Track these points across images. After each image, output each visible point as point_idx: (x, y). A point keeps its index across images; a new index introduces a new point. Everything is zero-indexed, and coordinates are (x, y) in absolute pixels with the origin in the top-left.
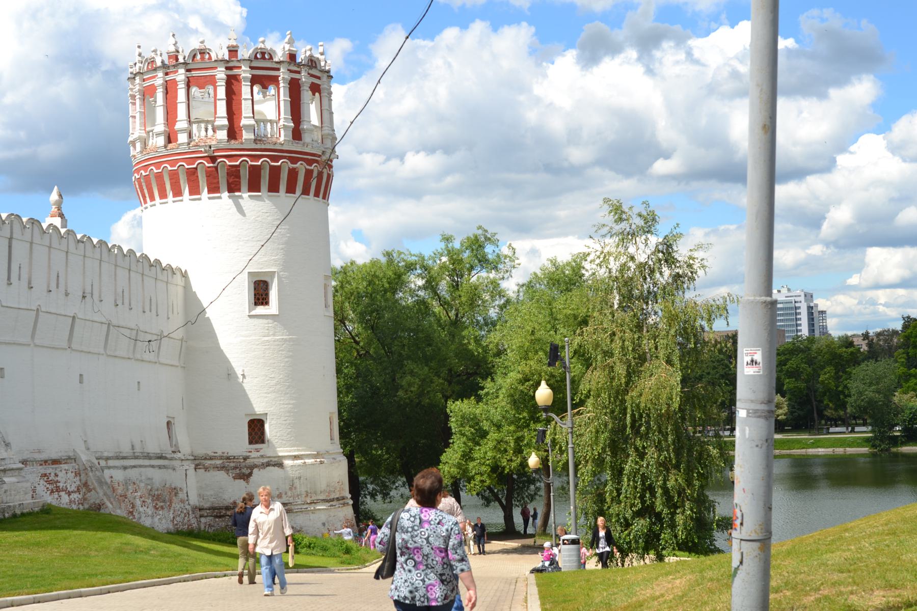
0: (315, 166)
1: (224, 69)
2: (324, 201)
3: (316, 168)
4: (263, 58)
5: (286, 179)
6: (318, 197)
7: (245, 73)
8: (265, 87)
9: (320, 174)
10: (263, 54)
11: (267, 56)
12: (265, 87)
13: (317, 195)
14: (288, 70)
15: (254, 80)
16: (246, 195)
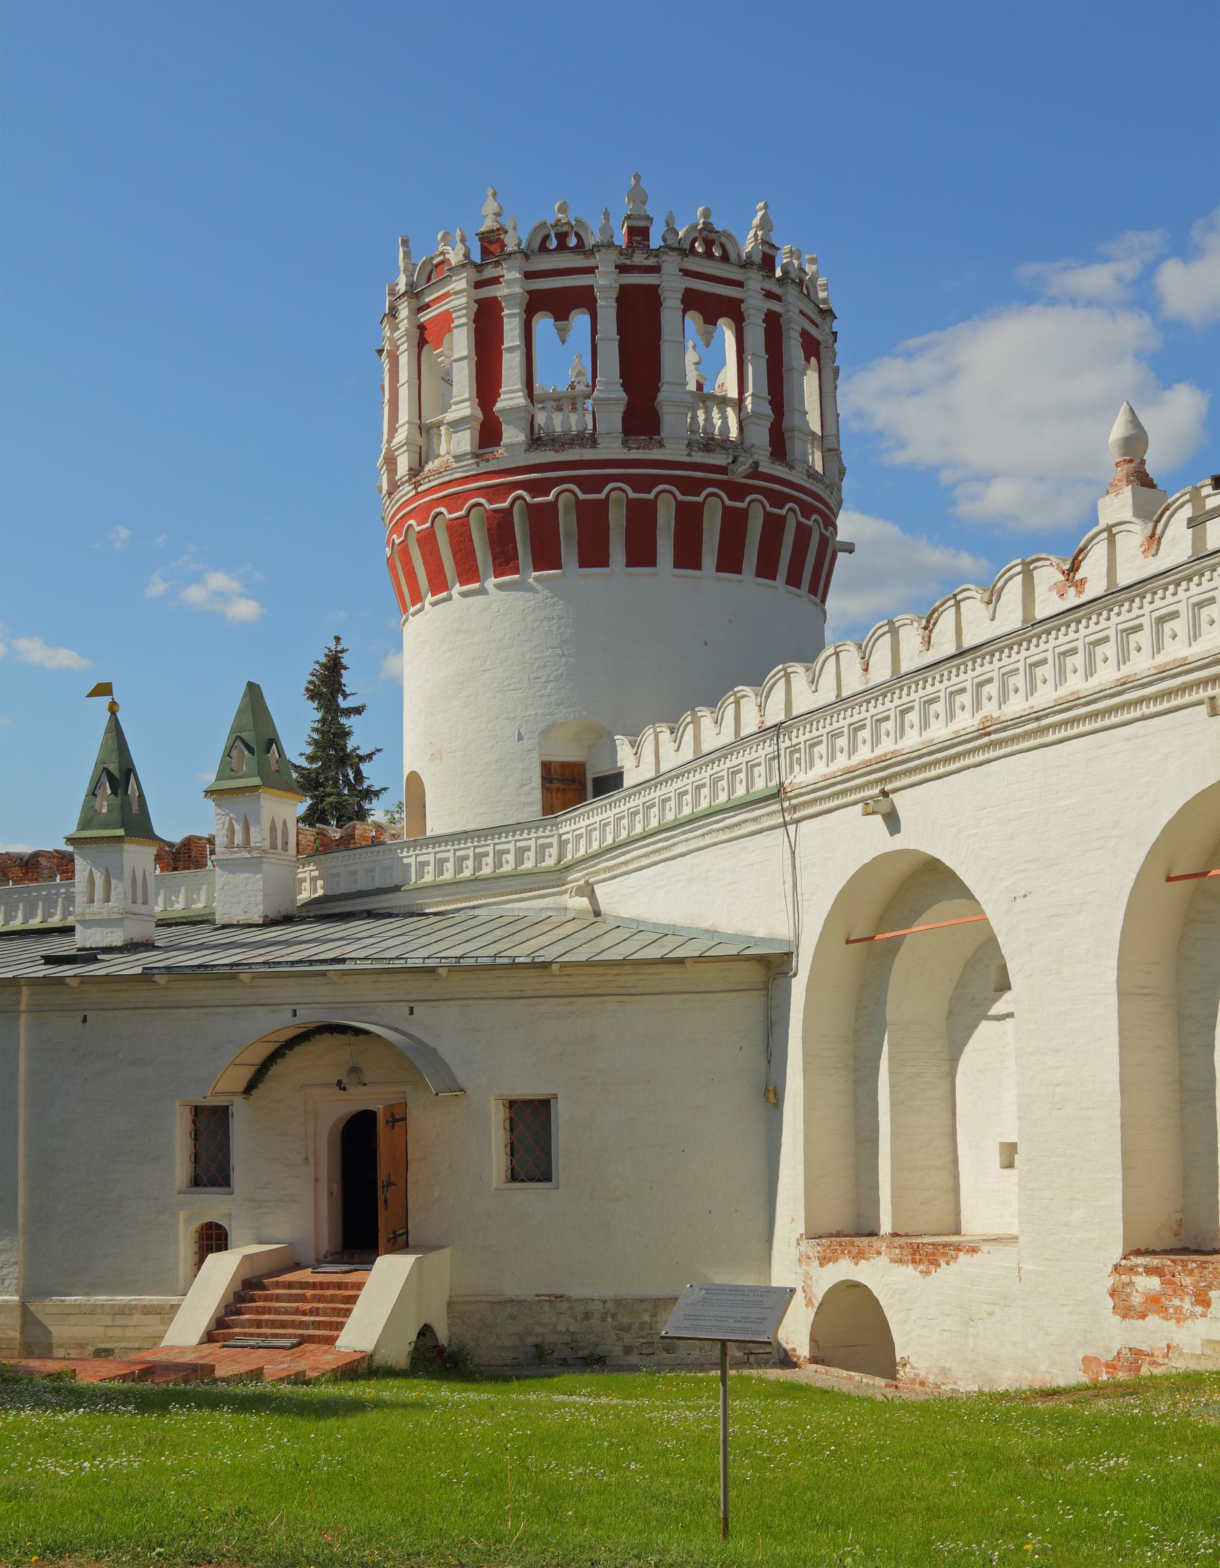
0: (790, 509)
1: (518, 275)
2: (813, 597)
3: (791, 514)
4: (562, 247)
5: (718, 538)
6: (798, 586)
7: (672, 285)
8: (561, 315)
9: (803, 533)
10: (562, 237)
11: (572, 242)
12: (561, 315)
13: (794, 579)
14: (681, 270)
15: (535, 304)
16: (491, 582)
